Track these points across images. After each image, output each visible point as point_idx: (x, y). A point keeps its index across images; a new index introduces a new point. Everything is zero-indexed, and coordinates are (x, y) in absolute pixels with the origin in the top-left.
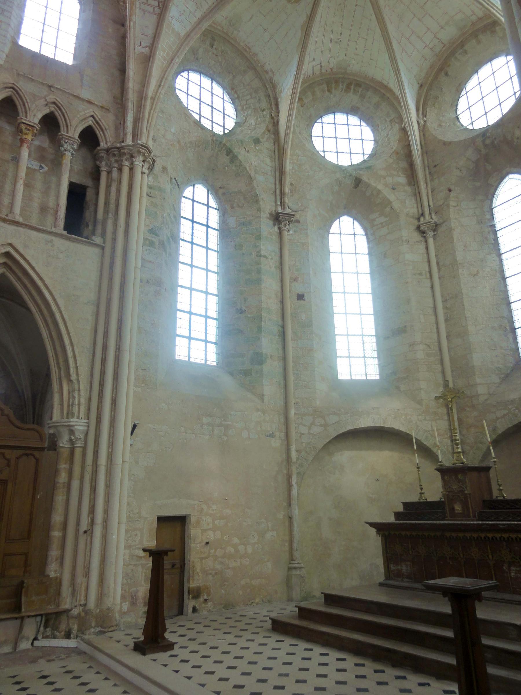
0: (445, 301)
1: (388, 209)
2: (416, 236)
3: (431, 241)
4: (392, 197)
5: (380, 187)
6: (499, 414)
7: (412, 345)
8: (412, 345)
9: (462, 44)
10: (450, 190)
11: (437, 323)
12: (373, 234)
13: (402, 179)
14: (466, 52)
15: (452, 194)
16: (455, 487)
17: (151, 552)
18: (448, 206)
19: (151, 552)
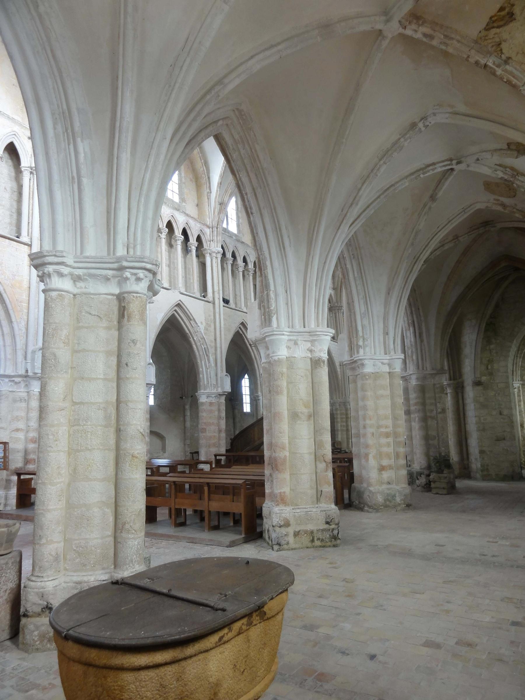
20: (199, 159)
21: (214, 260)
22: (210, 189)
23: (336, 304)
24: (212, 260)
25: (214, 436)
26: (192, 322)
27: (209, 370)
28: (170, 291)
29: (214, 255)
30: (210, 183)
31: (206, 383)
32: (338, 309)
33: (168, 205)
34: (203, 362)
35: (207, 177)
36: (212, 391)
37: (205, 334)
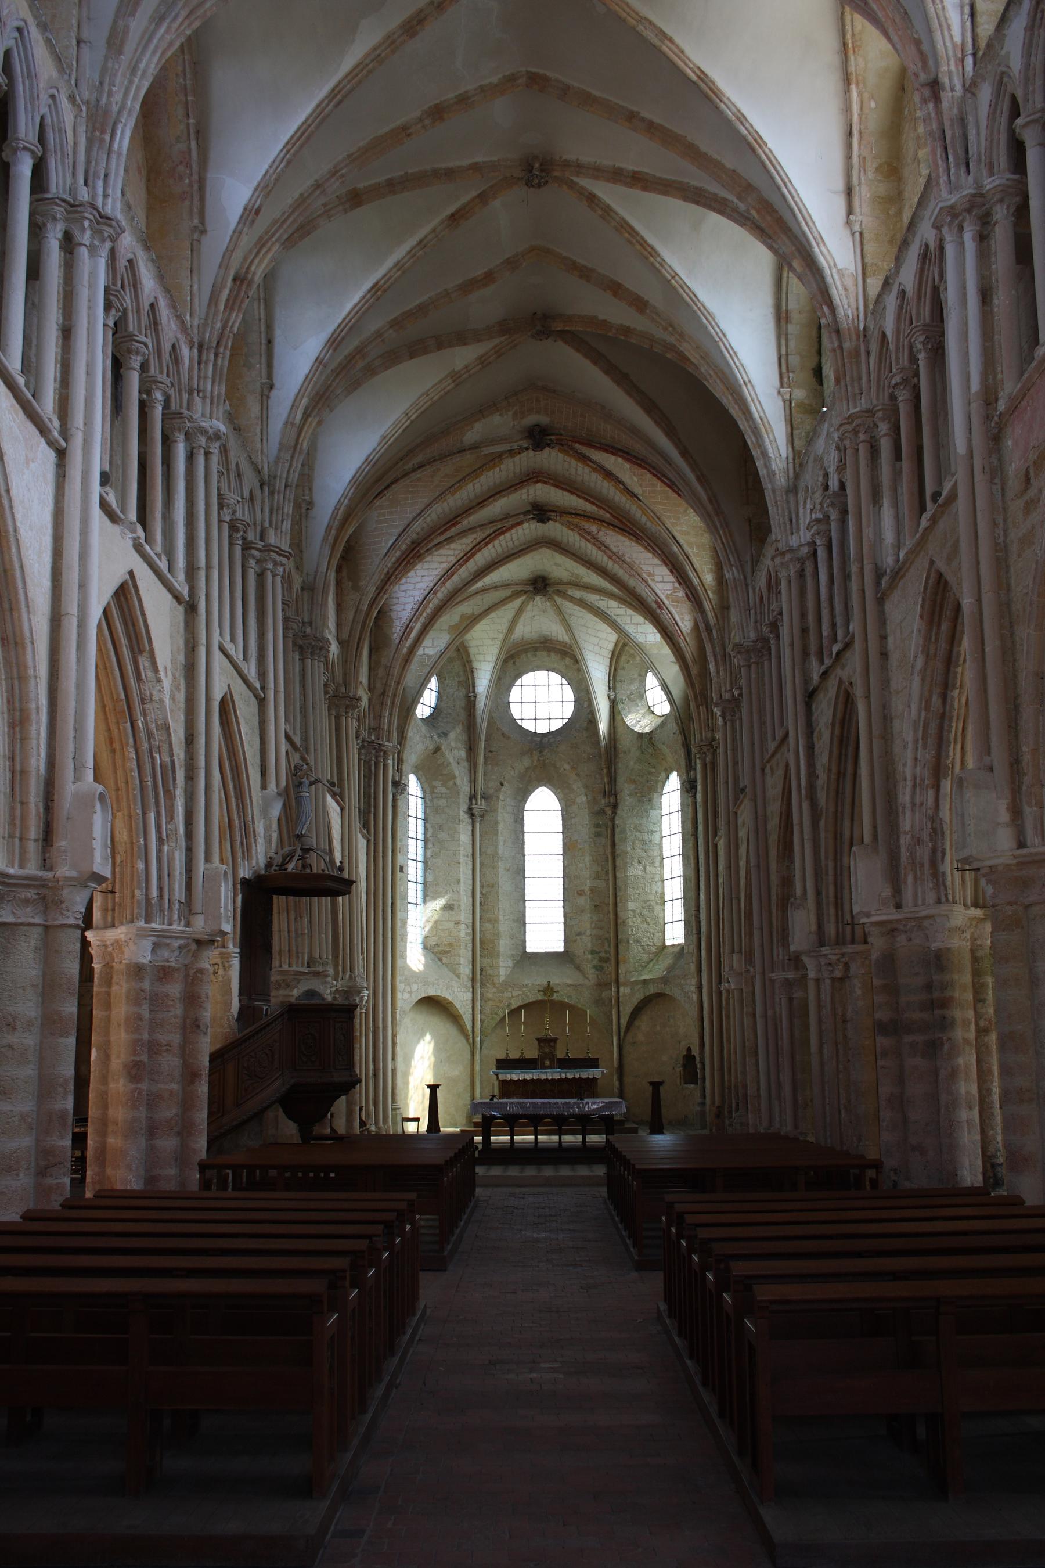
0: (482, 886)
1: (451, 783)
2: (464, 816)
3: (478, 825)
4: (457, 774)
5: (451, 760)
6: (515, 993)
7: (457, 923)
8: (457, 923)
9: (536, 649)
10: (502, 785)
11: (473, 905)
12: (432, 801)
13: (463, 754)
14: (536, 656)
15: (503, 789)
16: (547, 1050)
17: (429, 1086)
18: (498, 798)
19: (429, 1086)
20: (180, 112)
21: (201, 460)
22: (202, 222)
23: (343, 689)
24: (190, 457)
25: (171, 1092)
26: (144, 662)
27: (166, 848)
28: (116, 529)
29: (203, 440)
30: (202, 199)
31: (154, 893)
32: (347, 707)
33: (133, 218)
34: (152, 816)
35: (195, 177)
36: (175, 927)
37: (172, 711)
